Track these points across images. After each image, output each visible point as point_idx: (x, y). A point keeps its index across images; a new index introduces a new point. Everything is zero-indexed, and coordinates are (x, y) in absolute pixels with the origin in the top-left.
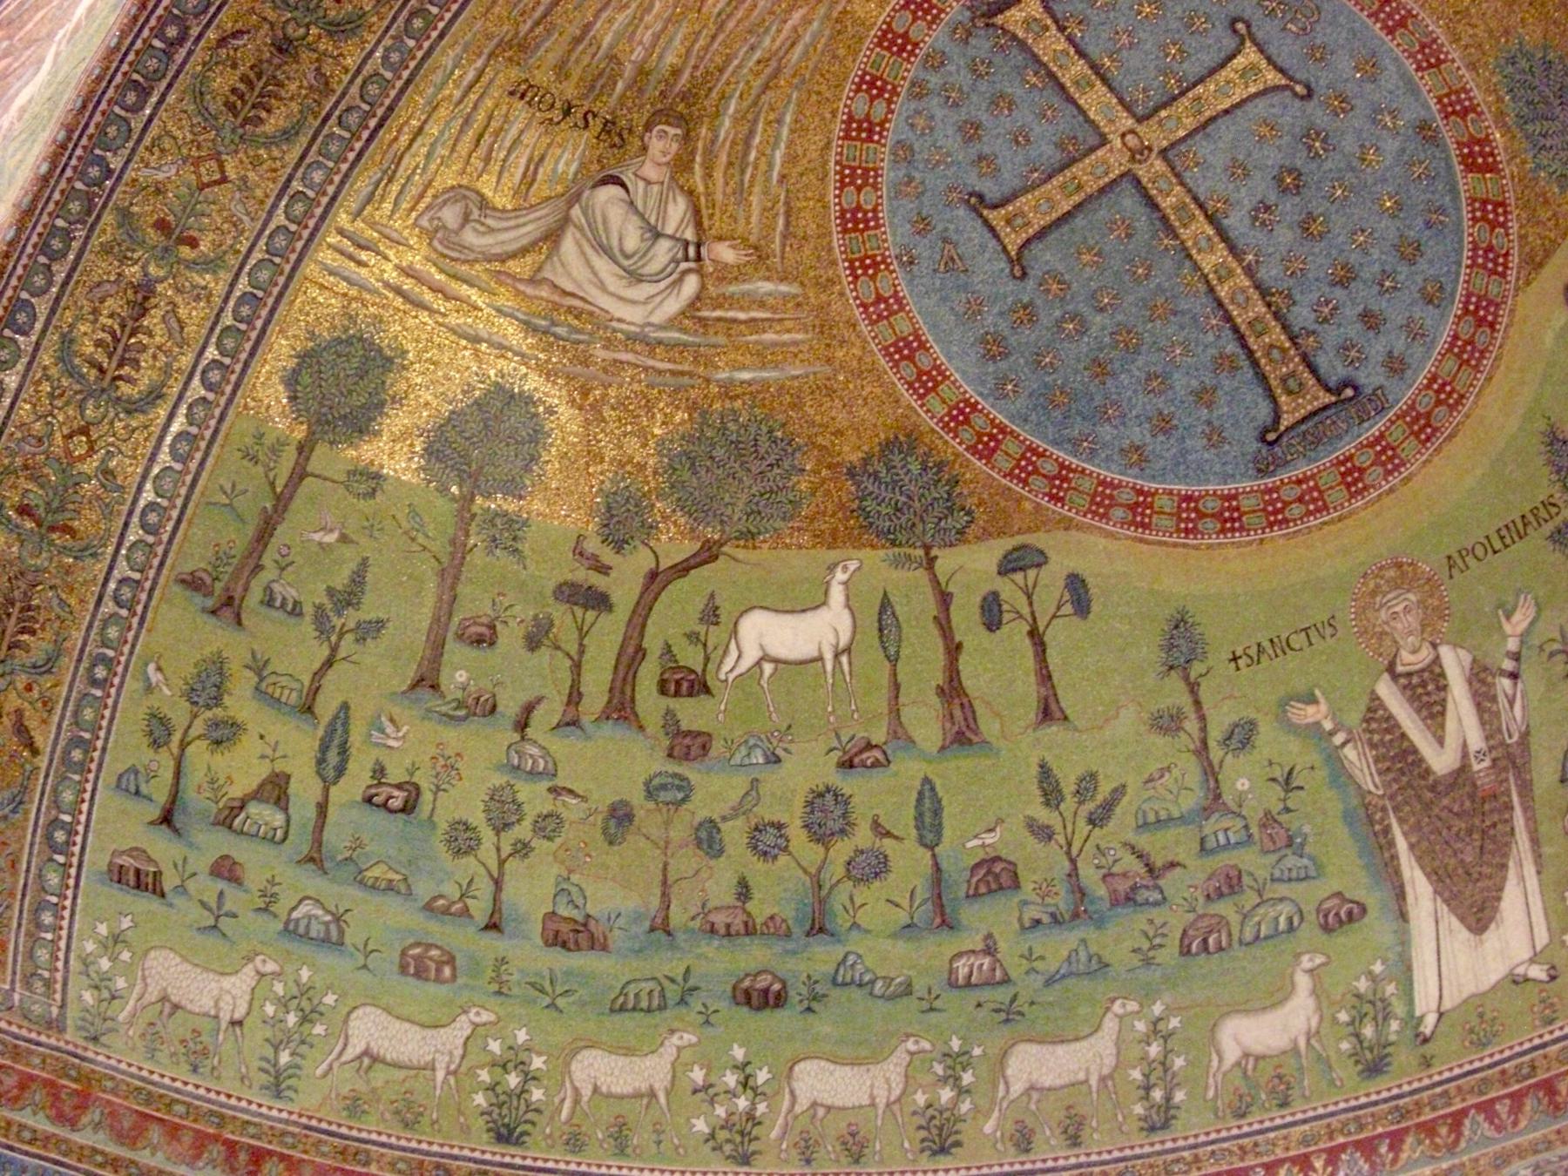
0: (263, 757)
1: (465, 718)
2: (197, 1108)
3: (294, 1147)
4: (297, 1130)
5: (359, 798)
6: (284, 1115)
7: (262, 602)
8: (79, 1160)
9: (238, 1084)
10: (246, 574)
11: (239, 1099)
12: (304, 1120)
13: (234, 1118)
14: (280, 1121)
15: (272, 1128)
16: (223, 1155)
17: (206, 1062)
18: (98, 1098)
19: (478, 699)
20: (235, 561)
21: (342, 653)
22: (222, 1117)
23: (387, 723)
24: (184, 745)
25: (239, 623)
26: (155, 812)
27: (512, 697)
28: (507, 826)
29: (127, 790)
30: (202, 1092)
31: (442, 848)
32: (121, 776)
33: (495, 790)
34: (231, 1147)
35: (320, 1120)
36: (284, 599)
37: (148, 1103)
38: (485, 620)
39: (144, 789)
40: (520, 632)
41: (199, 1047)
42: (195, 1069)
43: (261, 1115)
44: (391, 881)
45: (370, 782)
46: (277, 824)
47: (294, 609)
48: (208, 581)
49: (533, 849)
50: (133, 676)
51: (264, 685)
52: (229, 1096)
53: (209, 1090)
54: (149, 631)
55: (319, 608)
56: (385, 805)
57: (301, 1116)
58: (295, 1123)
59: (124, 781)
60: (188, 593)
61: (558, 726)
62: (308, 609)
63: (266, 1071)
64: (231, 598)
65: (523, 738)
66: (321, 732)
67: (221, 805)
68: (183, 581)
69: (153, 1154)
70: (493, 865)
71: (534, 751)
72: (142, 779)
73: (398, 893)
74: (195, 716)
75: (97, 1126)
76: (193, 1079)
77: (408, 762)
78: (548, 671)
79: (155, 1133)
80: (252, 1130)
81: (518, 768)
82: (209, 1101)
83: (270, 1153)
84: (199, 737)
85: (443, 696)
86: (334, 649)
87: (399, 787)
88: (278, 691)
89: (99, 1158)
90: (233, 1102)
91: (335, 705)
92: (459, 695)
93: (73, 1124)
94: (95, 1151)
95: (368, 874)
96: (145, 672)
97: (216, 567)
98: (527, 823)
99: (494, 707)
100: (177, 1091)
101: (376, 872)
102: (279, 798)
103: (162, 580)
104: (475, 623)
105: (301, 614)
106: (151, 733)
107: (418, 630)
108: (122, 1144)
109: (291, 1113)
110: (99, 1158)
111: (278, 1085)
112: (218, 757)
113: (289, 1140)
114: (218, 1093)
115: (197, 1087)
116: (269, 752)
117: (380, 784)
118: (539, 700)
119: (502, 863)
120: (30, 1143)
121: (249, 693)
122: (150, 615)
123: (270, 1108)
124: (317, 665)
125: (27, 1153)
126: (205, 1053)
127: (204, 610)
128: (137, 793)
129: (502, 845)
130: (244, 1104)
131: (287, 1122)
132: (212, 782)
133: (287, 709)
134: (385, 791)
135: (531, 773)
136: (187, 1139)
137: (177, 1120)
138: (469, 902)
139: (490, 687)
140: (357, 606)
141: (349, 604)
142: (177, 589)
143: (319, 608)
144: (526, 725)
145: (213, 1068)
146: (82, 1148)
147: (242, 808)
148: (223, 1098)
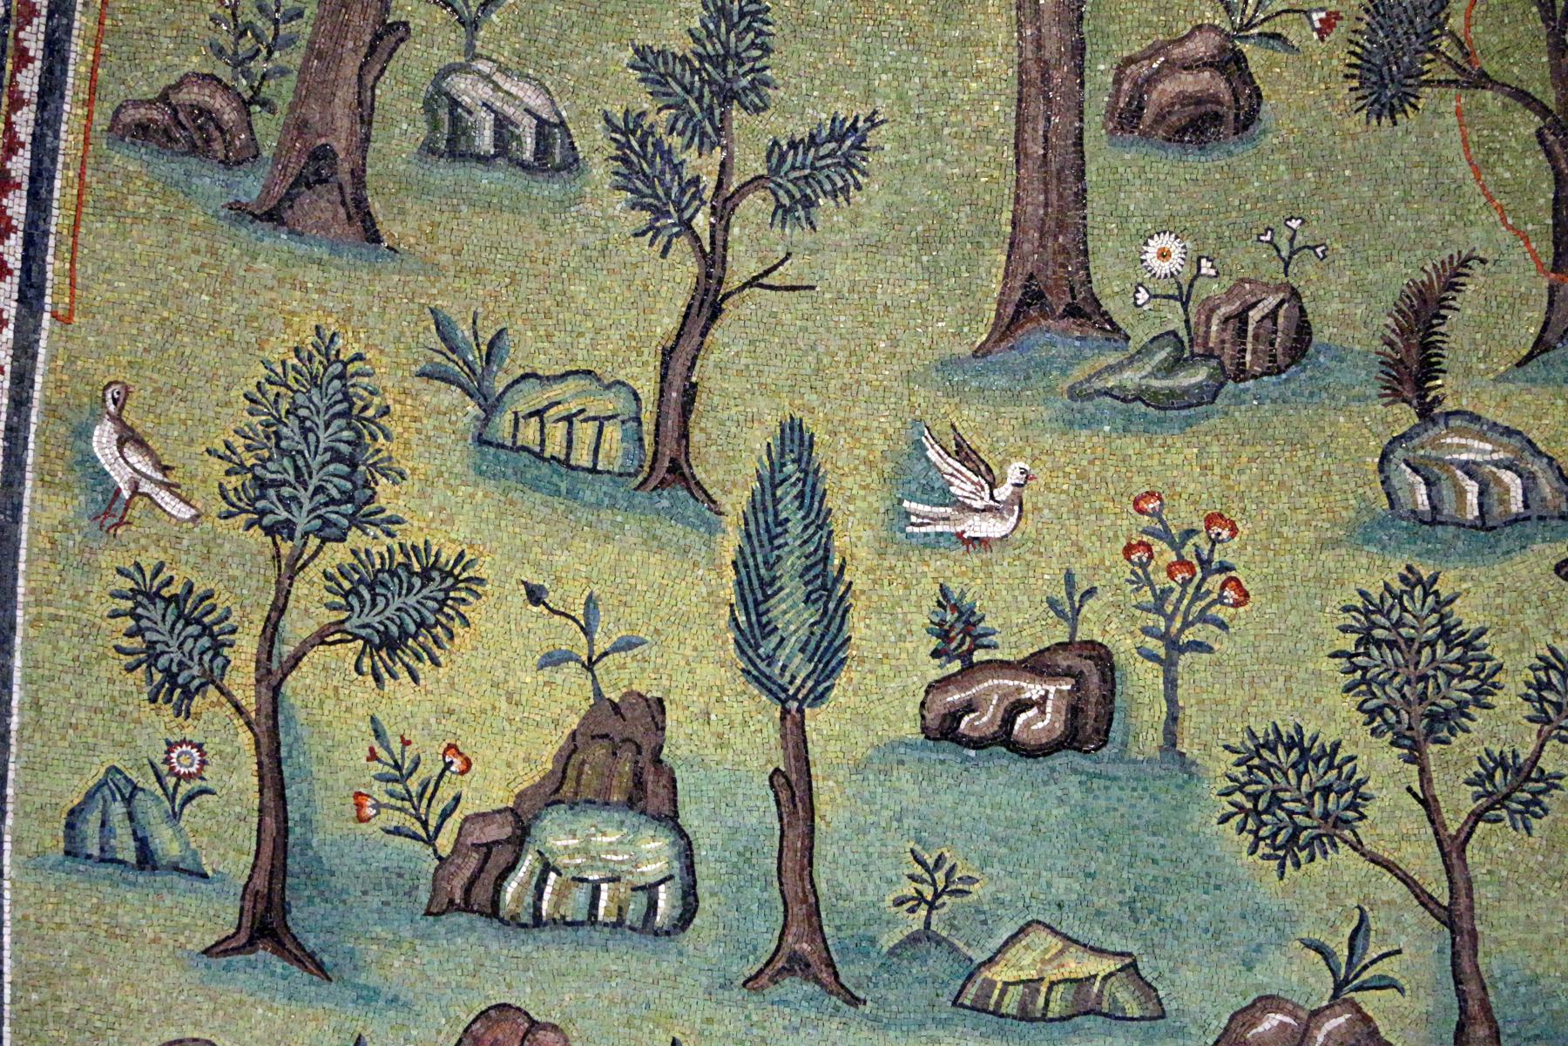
0: (553, 660)
1: (1208, 395)
5: (910, 730)
7: (429, 149)
10: (350, 68)
19: (1242, 317)
20: (303, 28)
21: (741, 265)
23: (949, 465)
24: (272, 676)
25: (374, 237)
26: (226, 916)
27: (1358, 286)
28: (1443, 722)
29: (107, 858)
31: (1232, 842)
32: (74, 817)
33: (1370, 608)
36: (502, 124)
38: (1200, 47)
39: (166, 843)
40: (1336, 54)
44: (1081, 983)
45: (934, 671)
46: (652, 870)
47: (543, 150)
48: (229, 116)
49: (1551, 782)
50: (44, 482)
51: (503, 425)
54: (63, 319)
55: (628, 130)
56: (1004, 738)
59: (91, 827)
60: (171, 167)
61: (1541, 345)
62: (594, 143)
64: (322, 155)
65: (1426, 413)
66: (730, 542)
67: (445, 843)
68: (143, 130)
70: (1423, 860)
71: (1479, 450)
72: (152, 811)
73: (1116, 1016)
74: (294, 568)
77: (1048, 581)
78: (1462, 170)
81: (1434, 519)
84: (321, 638)
85: (1114, 332)
86: (713, 260)
87: (1037, 665)
88: (558, 433)
91: (759, 440)
92: (1174, 318)
95: (1000, 974)
96: (88, 460)
97: (239, 63)
98: (1510, 700)
99: (1303, 330)
101: (1024, 962)
102: (639, 782)
103: (68, 139)
104: (1172, 66)
105: (572, 164)
106: (152, 654)
107: (984, 134)
112: (401, 689)
116: (570, 637)
117: (969, 667)
118: (1454, 274)
119: (1452, 850)
121: (459, 456)
122: (53, 266)
124: (669, 323)
127: (239, 211)
128: (146, 859)
129: (1438, 789)
132: (399, 773)
133: (604, 486)
134: (993, 690)
135: (1483, 523)
138: (1370, 1002)
139: (1272, 270)
140: (756, 95)
141: (728, 96)
142: (127, 160)
143: (628, 130)
144: (1428, 369)
147: (521, 837)
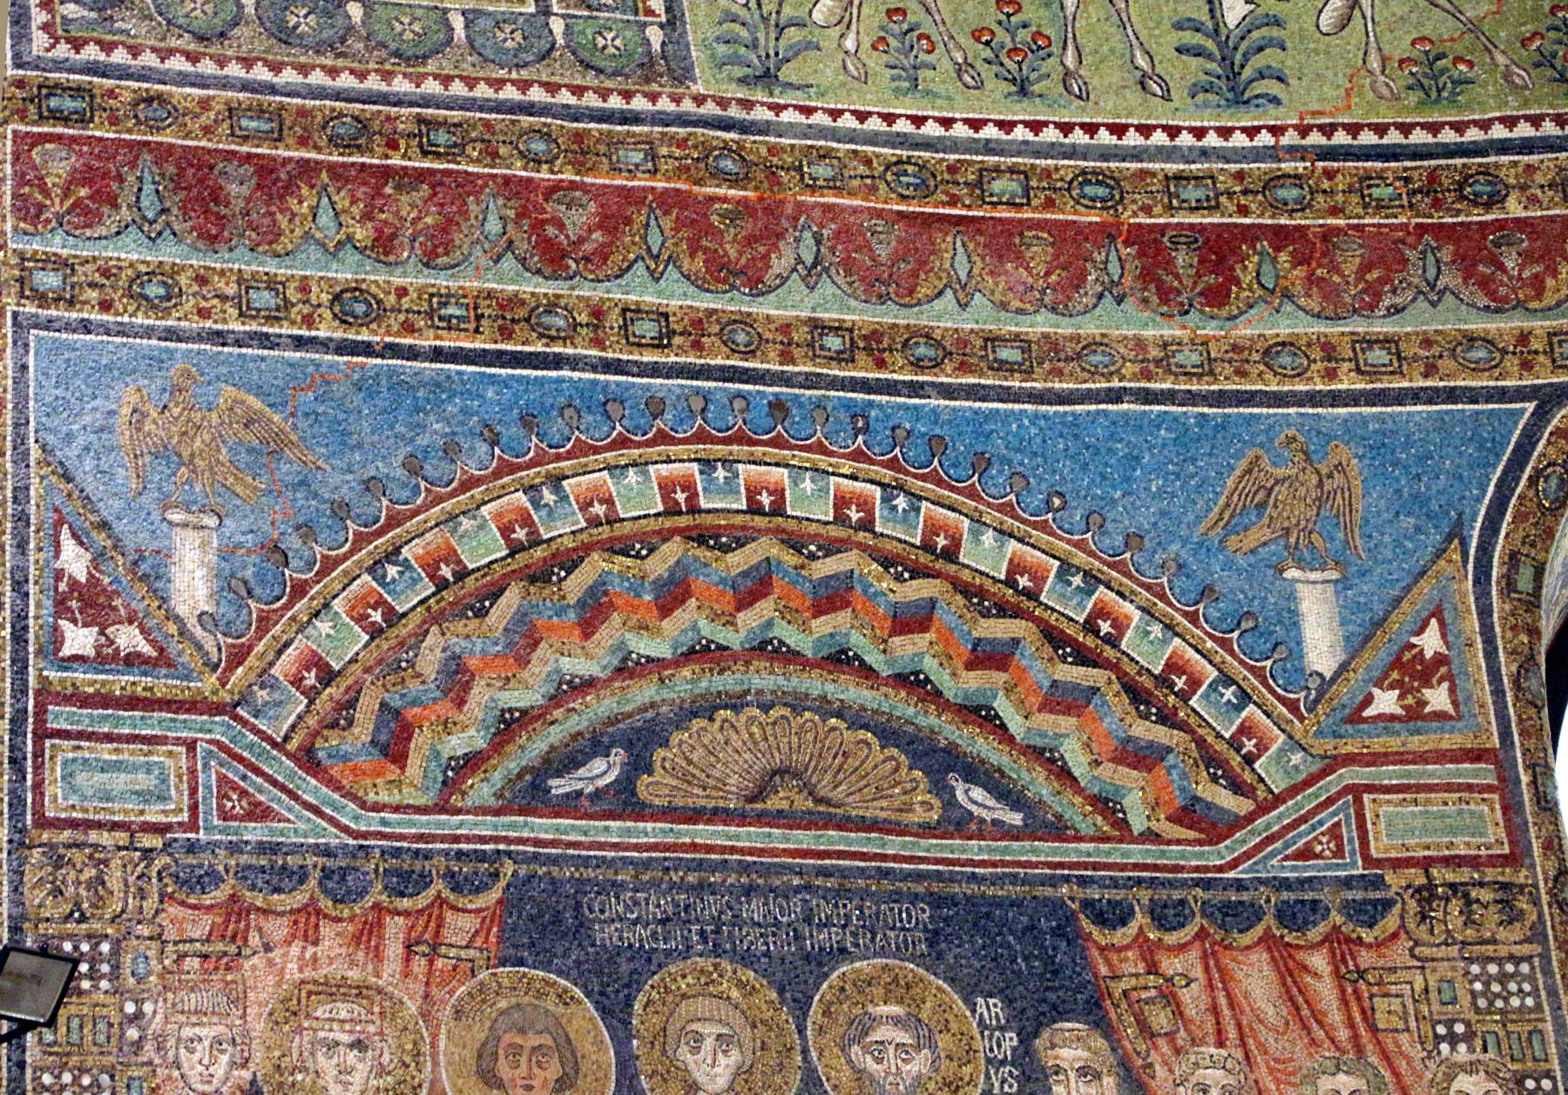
2: (1047, 173)
3: (1303, 207)
4: (1301, 166)
6: (1265, 139)
8: (787, 357)
9: (1134, 96)
11: (1145, 130)
12: (1315, 138)
13: (1143, 174)
14: (1258, 154)
15: (1240, 176)
16: (1133, 266)
17: (1046, 67)
18: (800, 208)
22: (1110, 180)
30: (1051, 135)
34: (1149, 243)
35: (1354, 130)
37: (924, 191)
41: (1023, 35)
42: (1023, 90)
43: (1205, 153)
52: (1119, 130)
53: (1066, 128)
57: (1304, 131)
58: (1295, 152)
63: (1199, 52)
69: (963, 306)
75: (813, 272)
76: (1021, 112)
79: (957, 256)
80: (1192, 193)
82: (1073, 152)
83: (1250, 235)
89: (834, 343)
90: (1132, 139)
93: (756, 284)
94: (817, 326)
100: (989, 147)
108: (882, 299)
109: (1276, 131)
110: (834, 343)
111: (1233, 74)
113: (1289, 193)
114: (1091, 129)
115: (1036, 127)
120: (658, 346)
123: (1225, 132)
125: (655, 370)
126: (1039, 45)
130: (1159, 138)
131: (1272, 153)
136: (1039, 253)
137: (1004, 213)
145: (1067, 73)
146: (786, 328)
148: (1104, 137)
